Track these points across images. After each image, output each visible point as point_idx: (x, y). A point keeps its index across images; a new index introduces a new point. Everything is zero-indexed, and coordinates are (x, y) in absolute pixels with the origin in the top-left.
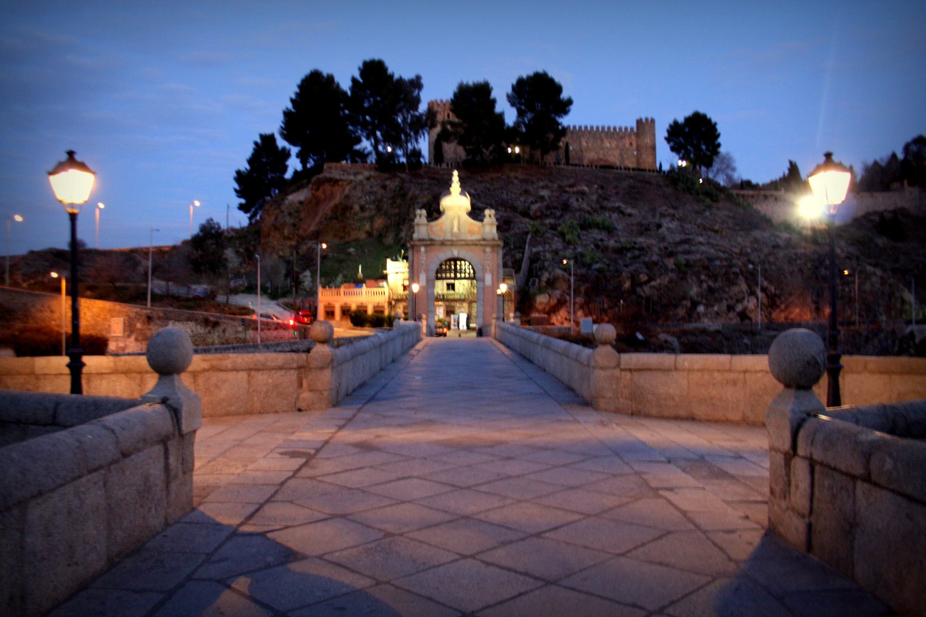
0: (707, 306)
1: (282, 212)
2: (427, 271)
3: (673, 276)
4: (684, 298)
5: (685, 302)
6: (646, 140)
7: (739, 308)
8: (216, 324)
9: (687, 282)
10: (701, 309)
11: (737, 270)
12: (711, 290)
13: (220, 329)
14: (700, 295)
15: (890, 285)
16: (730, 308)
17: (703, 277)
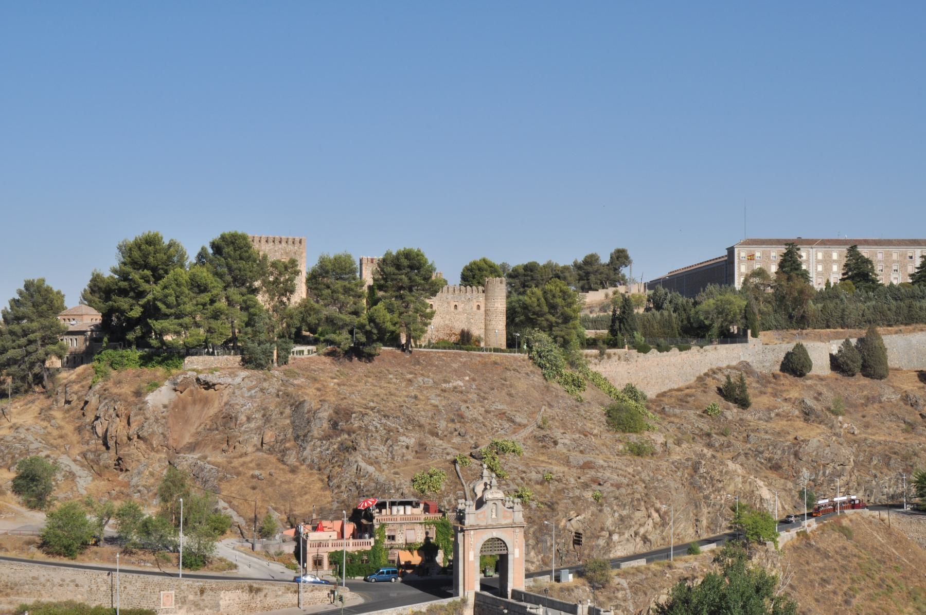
0: (621, 534)
1: (146, 419)
2: (474, 550)
3: (593, 508)
4: (602, 529)
5: (604, 533)
6: (496, 305)
7: (642, 531)
8: (258, 590)
9: (604, 514)
10: (615, 537)
11: (639, 496)
12: (622, 519)
13: (262, 594)
14: (614, 524)
15: (750, 483)
16: (636, 534)
17: (615, 508)
